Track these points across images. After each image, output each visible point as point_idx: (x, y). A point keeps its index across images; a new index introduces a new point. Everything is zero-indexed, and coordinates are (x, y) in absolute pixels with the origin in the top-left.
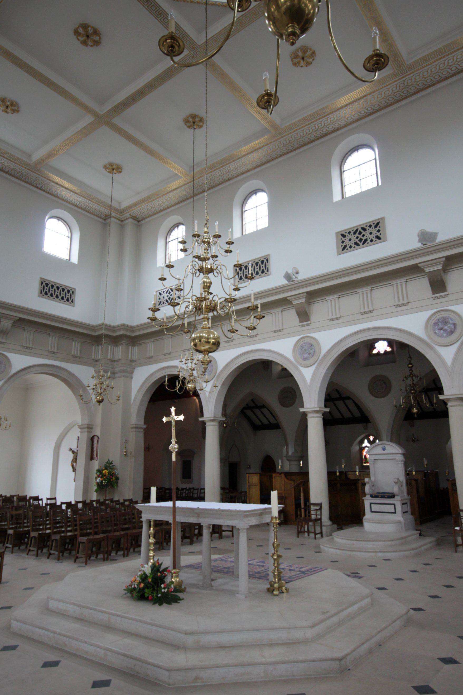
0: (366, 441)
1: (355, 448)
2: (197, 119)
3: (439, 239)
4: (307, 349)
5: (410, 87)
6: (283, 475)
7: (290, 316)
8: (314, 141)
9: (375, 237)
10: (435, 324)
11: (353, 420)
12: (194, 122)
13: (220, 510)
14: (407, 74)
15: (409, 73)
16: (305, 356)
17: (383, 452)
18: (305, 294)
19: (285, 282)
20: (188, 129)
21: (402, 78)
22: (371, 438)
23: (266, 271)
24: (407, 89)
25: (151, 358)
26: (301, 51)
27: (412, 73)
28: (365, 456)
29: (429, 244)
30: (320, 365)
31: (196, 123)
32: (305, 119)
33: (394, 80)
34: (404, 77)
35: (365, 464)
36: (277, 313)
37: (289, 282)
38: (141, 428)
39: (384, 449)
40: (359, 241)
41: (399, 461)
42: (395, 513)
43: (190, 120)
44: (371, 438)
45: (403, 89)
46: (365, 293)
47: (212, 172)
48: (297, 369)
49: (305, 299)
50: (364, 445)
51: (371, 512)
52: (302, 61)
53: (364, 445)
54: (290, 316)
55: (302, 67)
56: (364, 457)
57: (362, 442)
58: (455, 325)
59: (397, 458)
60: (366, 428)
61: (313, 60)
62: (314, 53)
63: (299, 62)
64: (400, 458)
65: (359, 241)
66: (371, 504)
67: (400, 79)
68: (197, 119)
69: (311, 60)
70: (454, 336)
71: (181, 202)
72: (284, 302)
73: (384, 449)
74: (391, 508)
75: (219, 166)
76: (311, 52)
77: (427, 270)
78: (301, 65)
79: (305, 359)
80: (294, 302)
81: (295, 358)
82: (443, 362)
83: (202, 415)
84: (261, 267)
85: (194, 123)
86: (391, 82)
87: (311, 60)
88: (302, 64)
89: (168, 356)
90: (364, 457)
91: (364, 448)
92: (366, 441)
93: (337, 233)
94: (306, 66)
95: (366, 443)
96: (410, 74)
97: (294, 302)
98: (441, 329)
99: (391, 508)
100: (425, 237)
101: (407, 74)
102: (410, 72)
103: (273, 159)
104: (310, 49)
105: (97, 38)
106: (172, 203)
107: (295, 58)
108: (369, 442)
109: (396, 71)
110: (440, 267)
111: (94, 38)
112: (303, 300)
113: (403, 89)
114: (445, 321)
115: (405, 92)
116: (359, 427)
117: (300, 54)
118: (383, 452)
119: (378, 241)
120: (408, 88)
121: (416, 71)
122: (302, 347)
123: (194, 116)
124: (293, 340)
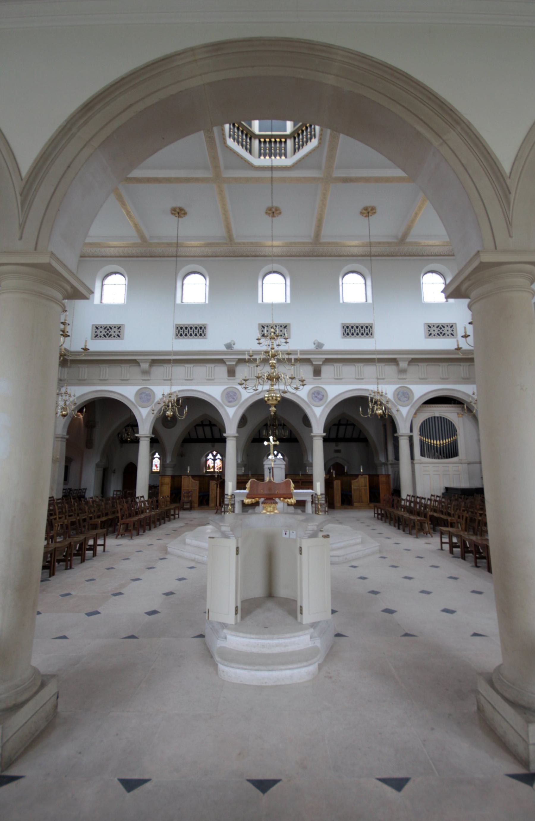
0: (210, 455)
1: (204, 459)
2: (183, 212)
4: (231, 396)
6: (190, 477)
7: (222, 370)
8: (249, 256)
10: (313, 393)
11: (205, 440)
12: (179, 212)
13: (304, 492)
16: (231, 399)
19: (224, 348)
23: (203, 335)
25: (84, 380)
29: (319, 350)
30: (240, 407)
32: (252, 243)
37: (227, 348)
38: (64, 438)
43: (178, 210)
48: (223, 407)
49: (231, 363)
54: (222, 370)
57: (208, 455)
58: (323, 396)
60: (213, 446)
63: (269, 214)
64: (283, 466)
70: (322, 402)
71: (126, 257)
72: (221, 361)
77: (314, 363)
79: (229, 402)
80: (227, 363)
81: (222, 400)
82: (315, 415)
83: (138, 433)
84: (199, 331)
89: (104, 381)
91: (208, 460)
92: (210, 455)
93: (259, 324)
95: (210, 456)
97: (227, 363)
98: (316, 397)
100: (319, 345)
103: (216, 256)
106: (118, 255)
108: (213, 455)
110: (321, 363)
112: (234, 363)
114: (318, 393)
116: (209, 445)
122: (228, 393)
123: (181, 209)
124: (223, 388)
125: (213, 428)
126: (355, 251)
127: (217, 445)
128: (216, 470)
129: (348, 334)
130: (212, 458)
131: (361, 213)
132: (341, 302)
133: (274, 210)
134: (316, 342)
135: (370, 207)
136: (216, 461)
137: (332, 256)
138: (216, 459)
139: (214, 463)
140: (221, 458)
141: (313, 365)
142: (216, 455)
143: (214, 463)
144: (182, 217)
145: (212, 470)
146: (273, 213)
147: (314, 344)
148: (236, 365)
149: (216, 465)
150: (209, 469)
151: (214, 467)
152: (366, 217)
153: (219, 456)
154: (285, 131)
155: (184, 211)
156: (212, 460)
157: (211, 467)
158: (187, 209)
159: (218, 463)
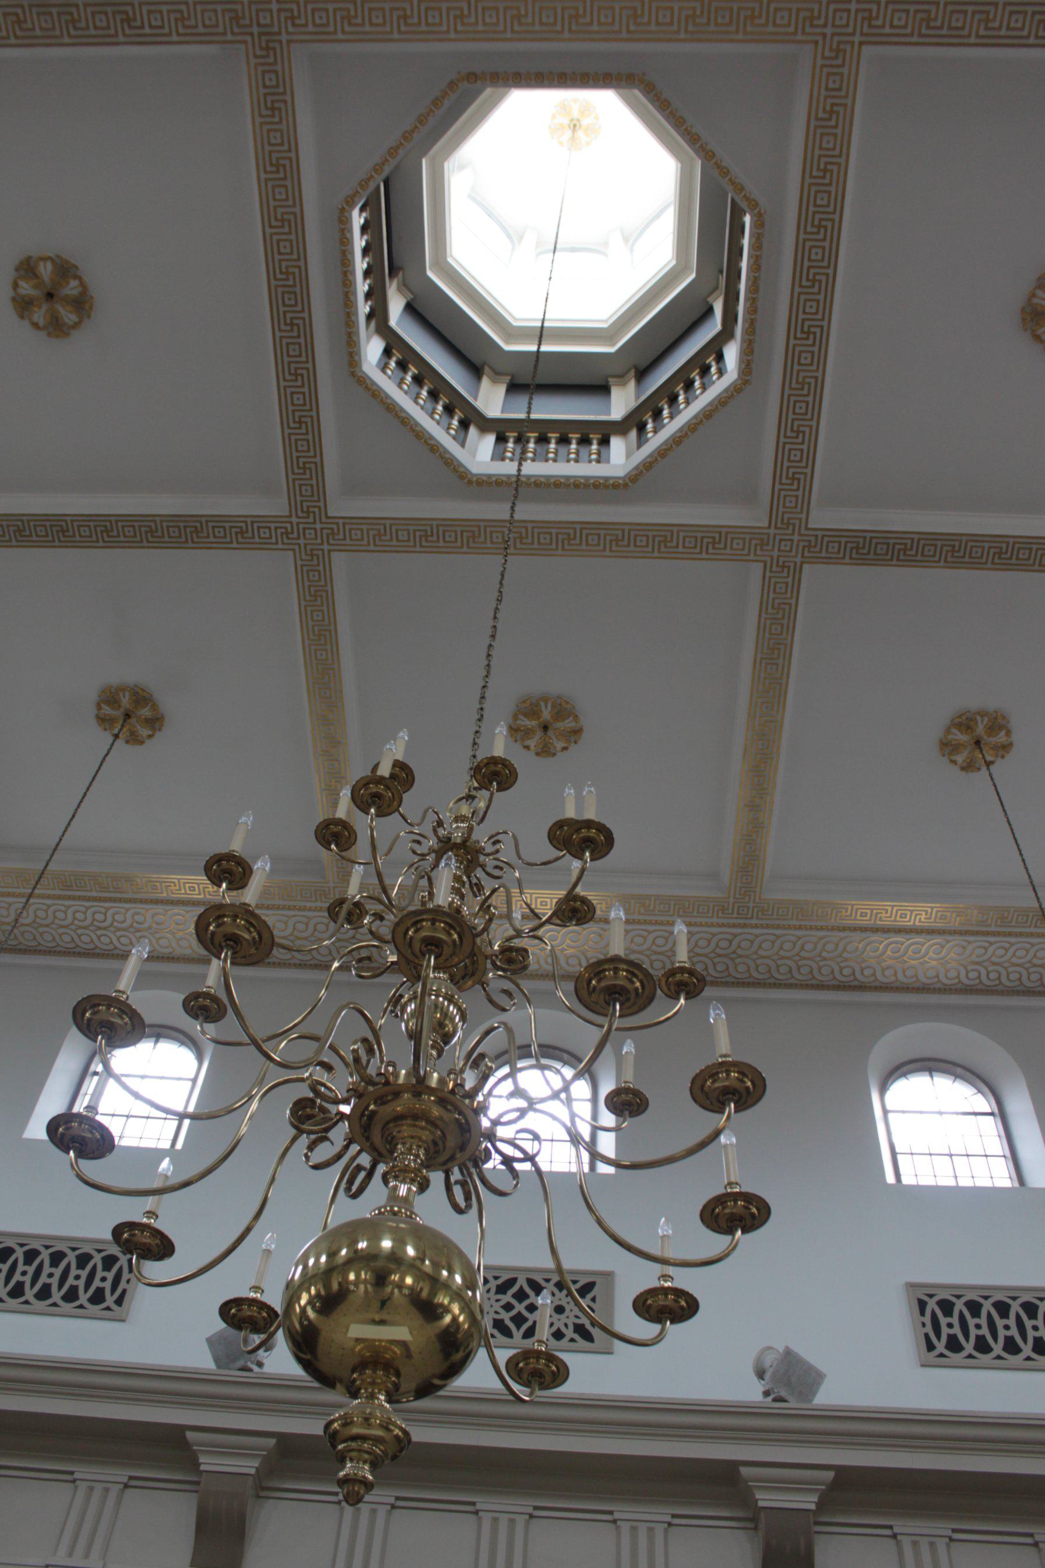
2: (146, 712)
3: (825, 1397)
5: (738, 961)
9: (571, 1327)
14: (748, 922)
15: (754, 921)
18: (272, 1442)
20: (93, 721)
21: (734, 926)
24: (729, 962)
26: (553, 706)
27: (762, 926)
31: (133, 720)
33: (715, 920)
34: (739, 926)
36: (99, 1487)
40: (512, 1319)
43: (125, 701)
45: (719, 956)
46: (504, 1519)
47: (59, 897)
52: (539, 734)
55: (527, 748)
61: (565, 749)
62: (577, 732)
63: (528, 733)
65: (512, 1319)
67: (729, 926)
68: (146, 712)
69: (559, 745)
75: (94, 894)
76: (573, 724)
78: (527, 743)
85: (127, 716)
86: (703, 920)
87: (559, 745)
88: (532, 743)
94: (537, 754)
96: (756, 926)
97: (208, 1463)
101: (748, 922)
102: (761, 922)
104: (576, 718)
105: (69, 317)
107: (526, 715)
109: (732, 900)
111: (60, 309)
112: (249, 1466)
113: (719, 956)
115: (720, 968)
117: (546, 714)
119: (582, 1343)
120: (732, 960)
121: (773, 927)
123: (141, 697)
126: (933, 958)
129: (954, 1345)
131: (948, 747)
132: (890, 1179)
133: (546, 714)
134: (769, 1360)
135: (983, 714)
137: (821, 987)
141: (753, 1517)
144: (134, 739)
146: (545, 728)
147: (760, 1374)
148: (263, 1485)
152: (968, 767)
154: (609, 414)
155: (154, 707)
158: (168, 703)
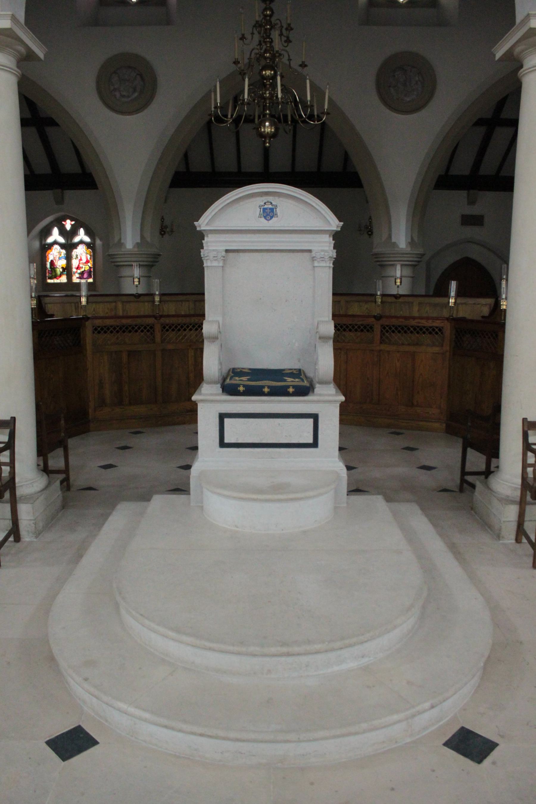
0: (56, 231)
17: (263, 224)
22: (68, 225)
28: (52, 263)
35: (49, 281)
39: (269, 213)
41: (322, 259)
42: (315, 444)
44: (68, 225)
50: (50, 240)
51: (223, 444)
53: (50, 240)
56: (48, 266)
57: (47, 232)
59: (315, 248)
60: (60, 201)
64: (325, 247)
66: (222, 417)
73: (269, 213)
74: (302, 431)
90: (48, 266)
92: (56, 231)
95: (55, 236)
99: (302, 431)
108: (63, 232)
118: (263, 224)
125: (50, 131)
127: (72, 196)
128: (75, 279)
130: (61, 240)
136: (75, 252)
138: (75, 246)
139: (69, 258)
140: (87, 239)
142: (74, 232)
143: (69, 258)
145: (64, 279)
149: (75, 263)
150: (56, 277)
151: (68, 270)
153: (82, 235)
156: (62, 246)
157: (59, 270)
159: (56, 255)
